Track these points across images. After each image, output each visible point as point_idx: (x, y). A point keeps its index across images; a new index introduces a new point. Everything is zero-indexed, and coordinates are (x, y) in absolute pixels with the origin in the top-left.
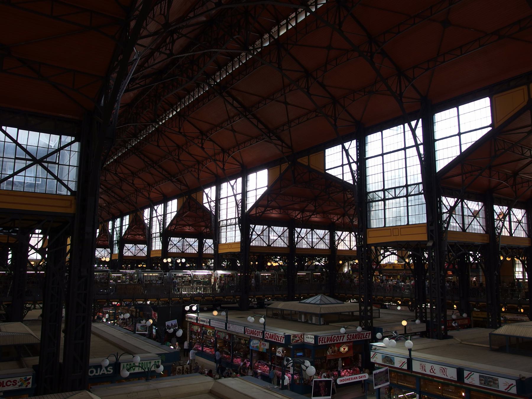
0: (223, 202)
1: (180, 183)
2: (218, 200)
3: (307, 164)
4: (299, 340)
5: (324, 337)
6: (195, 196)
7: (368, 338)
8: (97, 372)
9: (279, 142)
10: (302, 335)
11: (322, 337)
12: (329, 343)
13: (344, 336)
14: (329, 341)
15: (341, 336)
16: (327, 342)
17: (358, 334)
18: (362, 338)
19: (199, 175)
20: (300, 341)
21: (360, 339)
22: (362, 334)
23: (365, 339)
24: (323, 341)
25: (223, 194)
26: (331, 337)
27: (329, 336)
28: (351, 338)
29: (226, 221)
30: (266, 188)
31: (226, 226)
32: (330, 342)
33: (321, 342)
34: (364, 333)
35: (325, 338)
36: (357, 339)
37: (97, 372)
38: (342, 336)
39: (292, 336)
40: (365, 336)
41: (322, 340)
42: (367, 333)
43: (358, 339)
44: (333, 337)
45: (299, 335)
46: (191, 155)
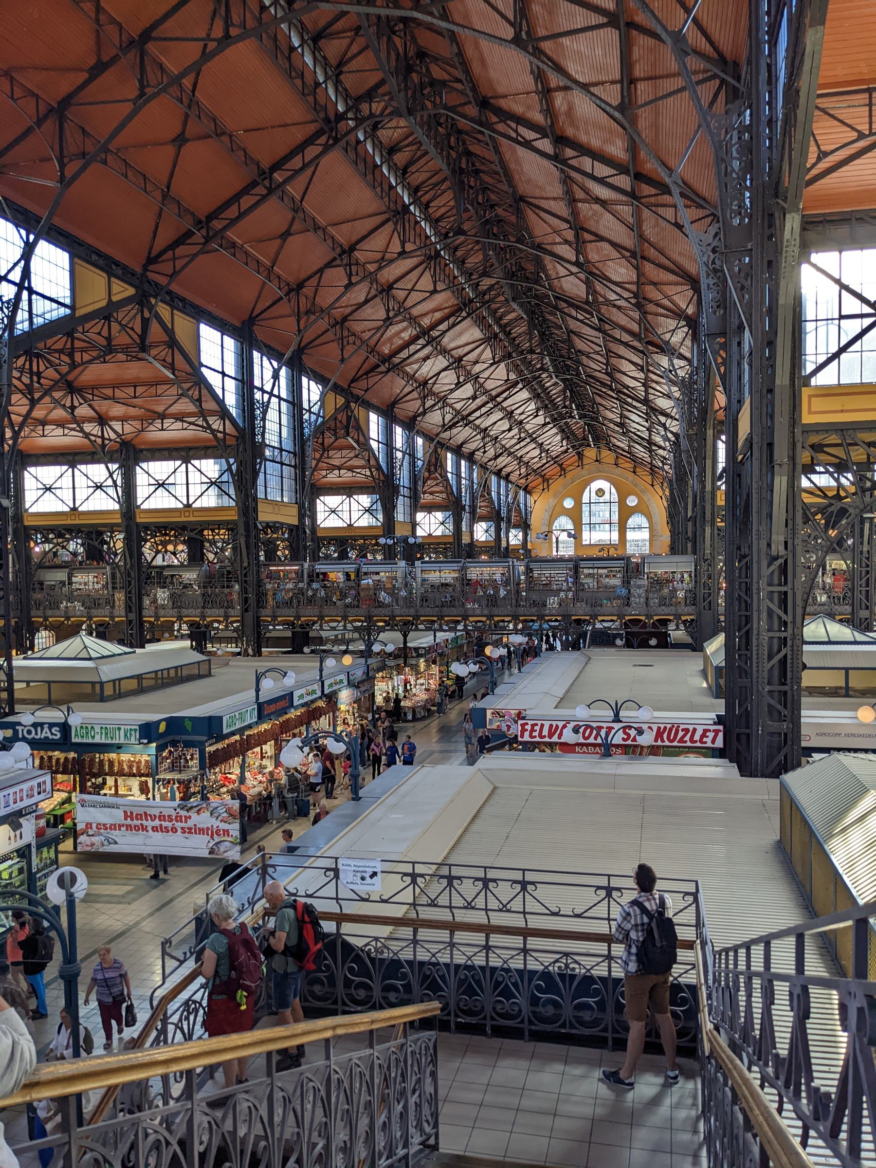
5: (539, 723)
7: (709, 744)
11: (530, 722)
13: (610, 729)
14: (556, 735)
16: (551, 735)
17: (671, 729)
21: (675, 744)
22: (687, 731)
23: (698, 744)
24: (535, 734)
33: (527, 734)
34: (695, 730)
35: (542, 725)
36: (663, 741)
39: (489, 712)
40: (697, 737)
41: (532, 730)
42: (705, 731)
43: (667, 743)
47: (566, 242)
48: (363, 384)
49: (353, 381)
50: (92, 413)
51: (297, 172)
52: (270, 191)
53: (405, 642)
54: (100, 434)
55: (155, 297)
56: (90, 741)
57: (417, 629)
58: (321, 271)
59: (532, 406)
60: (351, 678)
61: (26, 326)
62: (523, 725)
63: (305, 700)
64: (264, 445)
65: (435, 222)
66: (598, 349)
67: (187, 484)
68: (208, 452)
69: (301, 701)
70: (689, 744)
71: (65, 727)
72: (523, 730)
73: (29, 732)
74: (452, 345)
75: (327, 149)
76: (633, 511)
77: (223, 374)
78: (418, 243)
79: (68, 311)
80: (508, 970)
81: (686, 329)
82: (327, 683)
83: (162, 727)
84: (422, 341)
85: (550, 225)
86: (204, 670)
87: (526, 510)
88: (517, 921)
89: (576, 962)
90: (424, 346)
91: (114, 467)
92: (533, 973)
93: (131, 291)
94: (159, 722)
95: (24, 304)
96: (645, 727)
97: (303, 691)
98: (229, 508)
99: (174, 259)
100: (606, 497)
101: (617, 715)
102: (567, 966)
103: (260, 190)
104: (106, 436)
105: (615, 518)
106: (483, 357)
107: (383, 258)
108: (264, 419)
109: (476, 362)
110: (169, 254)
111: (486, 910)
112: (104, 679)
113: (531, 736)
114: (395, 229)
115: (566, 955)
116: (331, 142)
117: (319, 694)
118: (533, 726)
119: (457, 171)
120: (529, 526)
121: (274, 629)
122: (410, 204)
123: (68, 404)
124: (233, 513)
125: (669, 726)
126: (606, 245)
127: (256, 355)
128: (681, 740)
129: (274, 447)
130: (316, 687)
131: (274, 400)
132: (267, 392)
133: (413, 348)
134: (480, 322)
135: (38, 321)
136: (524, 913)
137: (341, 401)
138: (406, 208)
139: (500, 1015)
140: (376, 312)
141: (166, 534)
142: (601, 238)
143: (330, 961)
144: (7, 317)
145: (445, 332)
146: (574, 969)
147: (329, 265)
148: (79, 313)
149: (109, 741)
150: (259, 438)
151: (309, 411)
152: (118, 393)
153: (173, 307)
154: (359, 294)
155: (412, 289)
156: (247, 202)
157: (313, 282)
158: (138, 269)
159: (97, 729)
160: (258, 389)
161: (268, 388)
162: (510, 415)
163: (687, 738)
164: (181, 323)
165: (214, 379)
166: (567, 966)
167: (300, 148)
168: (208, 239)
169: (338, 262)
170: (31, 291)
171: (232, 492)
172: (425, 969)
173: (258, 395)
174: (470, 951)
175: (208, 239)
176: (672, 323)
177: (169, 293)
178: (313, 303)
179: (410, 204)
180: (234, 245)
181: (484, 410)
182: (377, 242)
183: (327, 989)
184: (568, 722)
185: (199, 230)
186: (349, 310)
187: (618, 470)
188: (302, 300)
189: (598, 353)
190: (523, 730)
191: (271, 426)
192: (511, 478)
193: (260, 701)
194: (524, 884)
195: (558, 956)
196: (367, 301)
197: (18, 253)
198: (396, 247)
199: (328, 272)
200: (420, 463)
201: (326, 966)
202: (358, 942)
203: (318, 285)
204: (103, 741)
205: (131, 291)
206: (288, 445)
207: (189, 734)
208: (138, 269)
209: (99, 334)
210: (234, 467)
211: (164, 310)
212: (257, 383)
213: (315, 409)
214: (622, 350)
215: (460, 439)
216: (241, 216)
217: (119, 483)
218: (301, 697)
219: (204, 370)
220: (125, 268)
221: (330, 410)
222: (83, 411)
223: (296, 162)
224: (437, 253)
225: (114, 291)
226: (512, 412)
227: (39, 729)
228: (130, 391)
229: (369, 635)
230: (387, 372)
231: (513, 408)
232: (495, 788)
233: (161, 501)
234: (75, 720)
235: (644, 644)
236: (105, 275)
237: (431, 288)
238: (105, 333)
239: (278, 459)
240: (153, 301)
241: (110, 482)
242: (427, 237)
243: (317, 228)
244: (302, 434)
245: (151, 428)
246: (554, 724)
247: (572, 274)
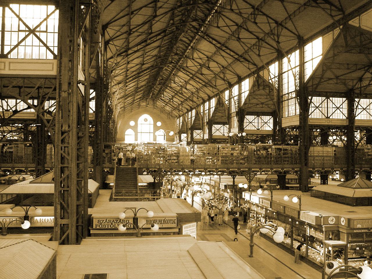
0: (285, 76)
1: (248, 63)
2: (280, 74)
3: (358, 25)
6: (262, 73)
9: (327, 6)
19: (259, 51)
25: (285, 68)
29: (287, 95)
30: (321, 57)
31: (288, 100)
46: (251, 32)
58: (141, 8)
66: (202, 56)
100: (148, 122)
105: (152, 131)
126: (265, 17)
133: (139, 47)
142: (264, 14)
189: (200, 59)
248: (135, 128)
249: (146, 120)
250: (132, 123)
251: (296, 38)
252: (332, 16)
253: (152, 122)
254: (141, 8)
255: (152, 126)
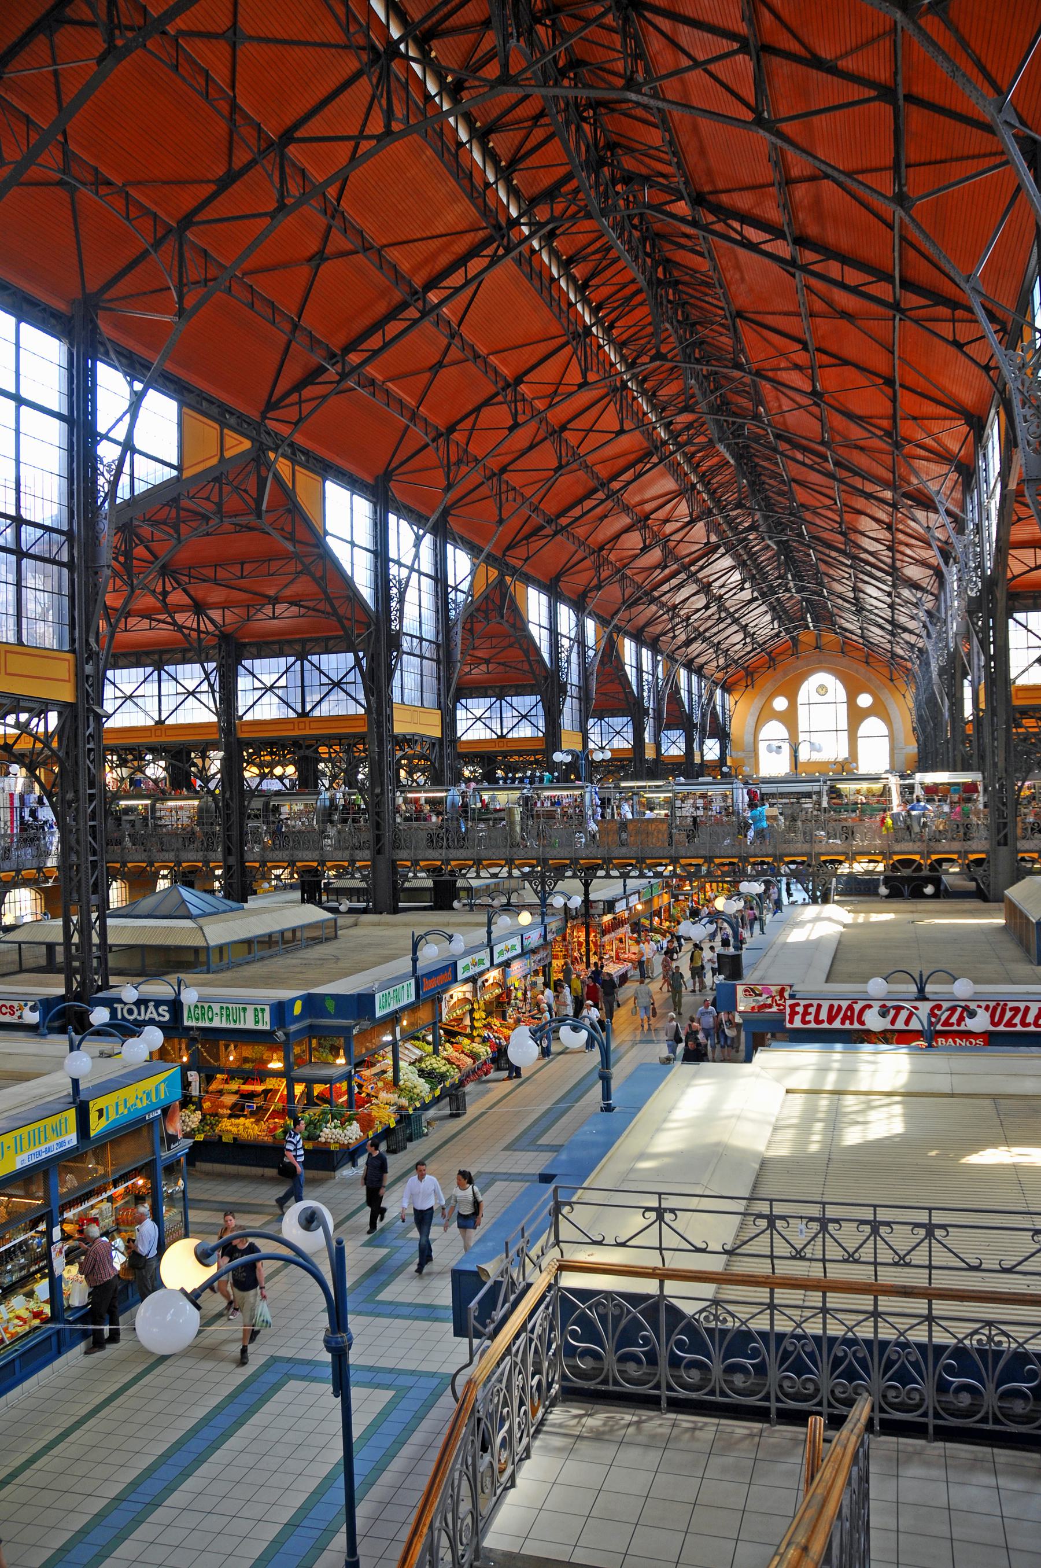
4: (770, 1006)
5: (815, 1003)
8: (139, 1014)
10: (781, 993)
11: (803, 1003)
12: (837, 1024)
14: (839, 1019)
15: (898, 1009)
16: (831, 1019)
18: (1015, 1025)
20: (775, 1009)
22: (1017, 1010)
23: (1032, 1028)
24: (808, 1018)
26: (850, 1008)
27: (841, 1003)
28: (954, 1020)
32: (843, 1023)
33: (798, 1019)
34: (1027, 1009)
35: (819, 1006)
37: (139, 1014)
38: (903, 1008)
40: (1030, 1019)
41: (806, 1013)
44: (857, 1007)
45: (773, 988)
47: (797, 367)
48: (521, 551)
49: (509, 547)
50: (187, 600)
51: (457, 290)
52: (424, 314)
53: (587, 894)
54: (195, 626)
55: (275, 450)
56: (207, 1024)
57: (608, 876)
58: (477, 409)
59: (737, 576)
60: (526, 942)
61: (127, 496)
62: (793, 1007)
63: (471, 973)
64: (400, 633)
65: (620, 346)
67: (303, 687)
68: (331, 643)
69: (467, 975)
70: (1019, 1028)
71: (176, 1006)
72: (793, 1013)
73: (130, 1012)
74: (637, 499)
75: (495, 260)
76: (866, 713)
77: (353, 544)
78: (601, 373)
79: (174, 473)
80: (905, 1345)
81: (954, 476)
82: (497, 949)
83: (298, 1009)
84: (600, 495)
85: (774, 347)
86: (330, 932)
87: (724, 713)
88: (917, 1278)
89: (1004, 1334)
90: (602, 501)
91: (211, 666)
92: (940, 1349)
93: (247, 444)
94: (293, 1001)
95: (126, 469)
96: (973, 1006)
97: (467, 960)
98: (355, 717)
99: (300, 402)
100: (829, 697)
101: (921, 990)
102: (990, 1338)
103: (412, 313)
104: (202, 628)
105: (843, 724)
106: (677, 513)
107: (555, 392)
108: (401, 601)
109: (667, 521)
110: (294, 397)
111: (824, 1260)
112: (212, 943)
113: (804, 1021)
114: (575, 352)
115: (989, 1323)
116: (501, 252)
117: (488, 964)
118: (806, 1007)
119: (654, 283)
120: (728, 735)
121: (415, 877)
122: (592, 325)
123: (159, 589)
124: (361, 723)
125: (992, 1004)
127: (392, 518)
128: (1009, 1024)
129: (412, 636)
130: (485, 954)
131: (415, 575)
132: (406, 567)
133: (588, 504)
134: (675, 469)
135: (140, 488)
136: (930, 1267)
137: (494, 574)
138: (587, 330)
139: (891, 1405)
140: (546, 456)
141: (274, 753)
142: (845, 362)
143: (649, 1333)
144: (109, 482)
145: (629, 483)
146: (1000, 1343)
147: (487, 402)
148: (187, 474)
149: (232, 1026)
150: (395, 626)
151: (456, 589)
152: (221, 574)
153: (294, 462)
154: (523, 437)
155: (591, 430)
156: (393, 328)
157: (467, 424)
158: (256, 416)
159: (216, 1007)
160: (393, 561)
161: (407, 560)
162: (706, 588)
163: (1017, 1020)
164: (304, 481)
165: (340, 551)
166: (990, 1338)
167: (462, 261)
168: (343, 376)
169: (500, 398)
170: (134, 451)
171: (361, 697)
172: (786, 1343)
173: (393, 570)
174: (851, 1319)
175: (343, 376)
176: (936, 469)
177: (291, 445)
178: (466, 451)
179: (592, 325)
180: (372, 382)
181: (674, 582)
182: (549, 371)
183: (645, 1369)
184: (855, 1001)
185: (333, 365)
186: (509, 458)
187: (845, 660)
188: (453, 448)
190: (793, 1013)
191: (410, 610)
192: (706, 671)
193: (419, 973)
194: (875, 1226)
195: (977, 1325)
196: (531, 447)
197: (126, 405)
198: (574, 376)
199: (486, 411)
200: (591, 653)
201: (644, 1338)
202: (688, 1308)
203: (473, 428)
204: (224, 1025)
205: (247, 444)
206: (429, 631)
207: (330, 1017)
208: (256, 416)
209: (208, 499)
210: (364, 663)
211: (283, 467)
212: (393, 554)
213: (465, 586)
214: (860, 503)
215: (641, 620)
216: (386, 345)
217: (217, 688)
218: (466, 968)
219: (329, 539)
220: (240, 417)
221: (481, 588)
222: (177, 597)
223: (456, 279)
224: (624, 384)
225: (227, 445)
226: (710, 584)
227: (143, 1008)
228: (236, 569)
229: (543, 884)
230: (554, 535)
231: (711, 579)
232: (788, 1091)
233: (268, 710)
234: (190, 996)
235: (917, 894)
236: (217, 426)
237: (617, 427)
238: (215, 498)
239: (417, 652)
240: (272, 455)
241: (205, 687)
242: (612, 365)
243: (477, 356)
244: (447, 618)
245: (260, 616)
246: (836, 1003)
247: (800, 407)
248: (789, 719)
249: (822, 689)
250: (780, 703)
251: (959, 423)
252: (959, 346)
253: (842, 695)
254: (477, 409)
255: (843, 709)
